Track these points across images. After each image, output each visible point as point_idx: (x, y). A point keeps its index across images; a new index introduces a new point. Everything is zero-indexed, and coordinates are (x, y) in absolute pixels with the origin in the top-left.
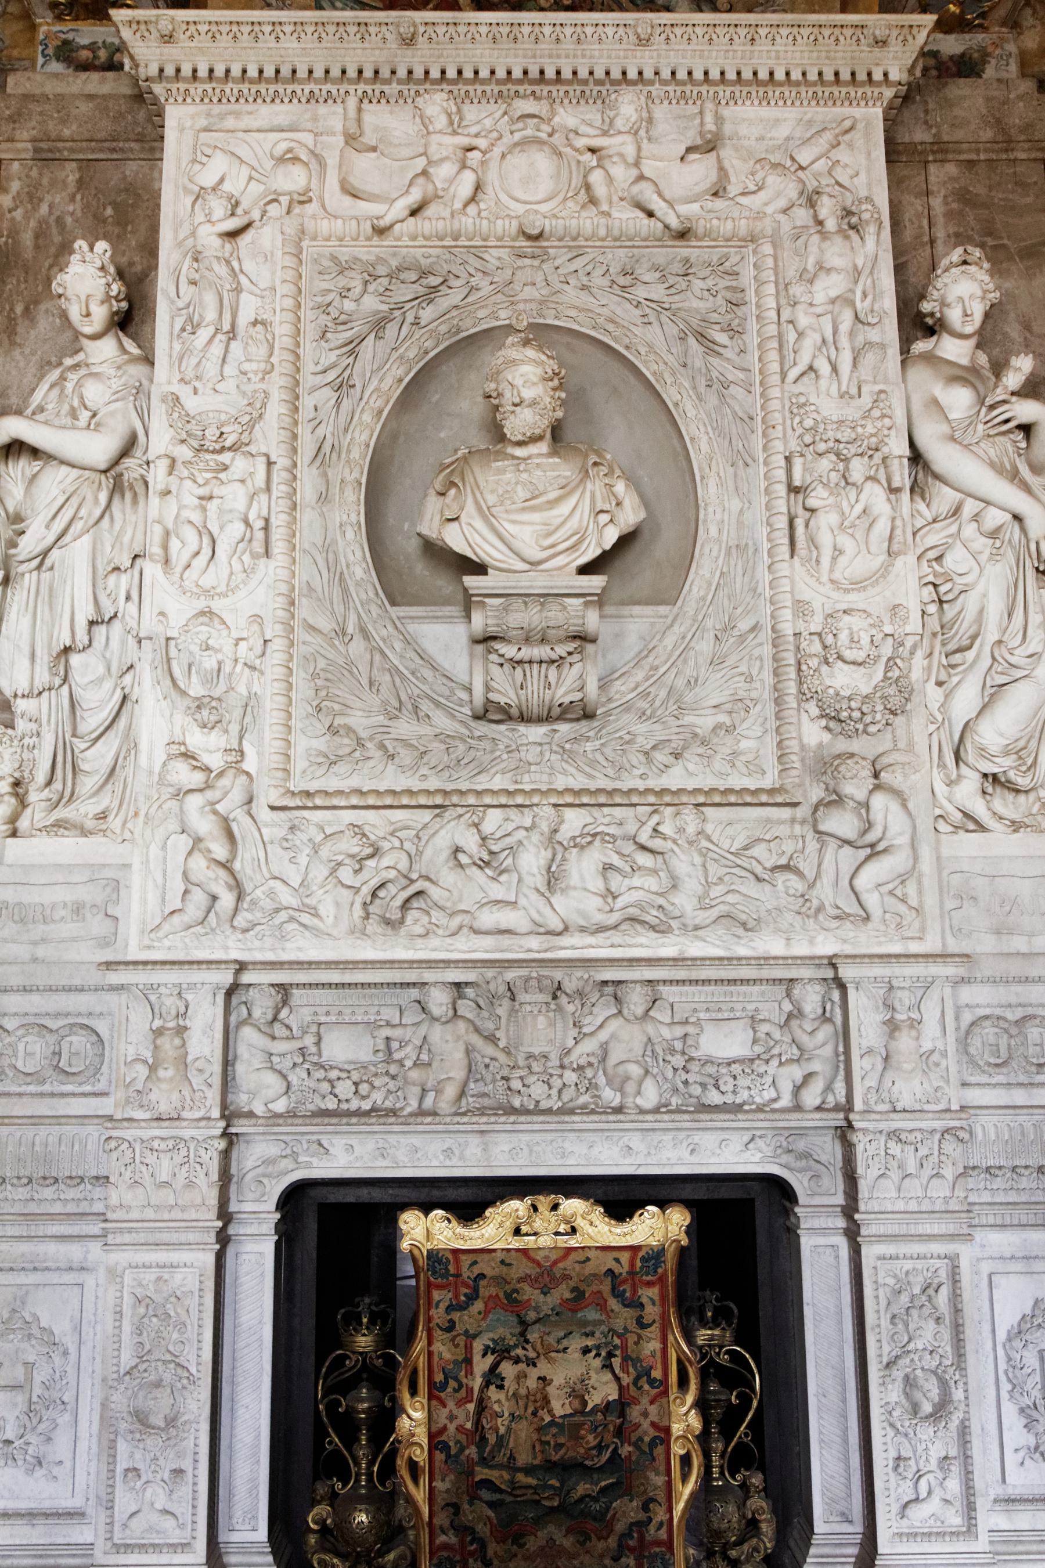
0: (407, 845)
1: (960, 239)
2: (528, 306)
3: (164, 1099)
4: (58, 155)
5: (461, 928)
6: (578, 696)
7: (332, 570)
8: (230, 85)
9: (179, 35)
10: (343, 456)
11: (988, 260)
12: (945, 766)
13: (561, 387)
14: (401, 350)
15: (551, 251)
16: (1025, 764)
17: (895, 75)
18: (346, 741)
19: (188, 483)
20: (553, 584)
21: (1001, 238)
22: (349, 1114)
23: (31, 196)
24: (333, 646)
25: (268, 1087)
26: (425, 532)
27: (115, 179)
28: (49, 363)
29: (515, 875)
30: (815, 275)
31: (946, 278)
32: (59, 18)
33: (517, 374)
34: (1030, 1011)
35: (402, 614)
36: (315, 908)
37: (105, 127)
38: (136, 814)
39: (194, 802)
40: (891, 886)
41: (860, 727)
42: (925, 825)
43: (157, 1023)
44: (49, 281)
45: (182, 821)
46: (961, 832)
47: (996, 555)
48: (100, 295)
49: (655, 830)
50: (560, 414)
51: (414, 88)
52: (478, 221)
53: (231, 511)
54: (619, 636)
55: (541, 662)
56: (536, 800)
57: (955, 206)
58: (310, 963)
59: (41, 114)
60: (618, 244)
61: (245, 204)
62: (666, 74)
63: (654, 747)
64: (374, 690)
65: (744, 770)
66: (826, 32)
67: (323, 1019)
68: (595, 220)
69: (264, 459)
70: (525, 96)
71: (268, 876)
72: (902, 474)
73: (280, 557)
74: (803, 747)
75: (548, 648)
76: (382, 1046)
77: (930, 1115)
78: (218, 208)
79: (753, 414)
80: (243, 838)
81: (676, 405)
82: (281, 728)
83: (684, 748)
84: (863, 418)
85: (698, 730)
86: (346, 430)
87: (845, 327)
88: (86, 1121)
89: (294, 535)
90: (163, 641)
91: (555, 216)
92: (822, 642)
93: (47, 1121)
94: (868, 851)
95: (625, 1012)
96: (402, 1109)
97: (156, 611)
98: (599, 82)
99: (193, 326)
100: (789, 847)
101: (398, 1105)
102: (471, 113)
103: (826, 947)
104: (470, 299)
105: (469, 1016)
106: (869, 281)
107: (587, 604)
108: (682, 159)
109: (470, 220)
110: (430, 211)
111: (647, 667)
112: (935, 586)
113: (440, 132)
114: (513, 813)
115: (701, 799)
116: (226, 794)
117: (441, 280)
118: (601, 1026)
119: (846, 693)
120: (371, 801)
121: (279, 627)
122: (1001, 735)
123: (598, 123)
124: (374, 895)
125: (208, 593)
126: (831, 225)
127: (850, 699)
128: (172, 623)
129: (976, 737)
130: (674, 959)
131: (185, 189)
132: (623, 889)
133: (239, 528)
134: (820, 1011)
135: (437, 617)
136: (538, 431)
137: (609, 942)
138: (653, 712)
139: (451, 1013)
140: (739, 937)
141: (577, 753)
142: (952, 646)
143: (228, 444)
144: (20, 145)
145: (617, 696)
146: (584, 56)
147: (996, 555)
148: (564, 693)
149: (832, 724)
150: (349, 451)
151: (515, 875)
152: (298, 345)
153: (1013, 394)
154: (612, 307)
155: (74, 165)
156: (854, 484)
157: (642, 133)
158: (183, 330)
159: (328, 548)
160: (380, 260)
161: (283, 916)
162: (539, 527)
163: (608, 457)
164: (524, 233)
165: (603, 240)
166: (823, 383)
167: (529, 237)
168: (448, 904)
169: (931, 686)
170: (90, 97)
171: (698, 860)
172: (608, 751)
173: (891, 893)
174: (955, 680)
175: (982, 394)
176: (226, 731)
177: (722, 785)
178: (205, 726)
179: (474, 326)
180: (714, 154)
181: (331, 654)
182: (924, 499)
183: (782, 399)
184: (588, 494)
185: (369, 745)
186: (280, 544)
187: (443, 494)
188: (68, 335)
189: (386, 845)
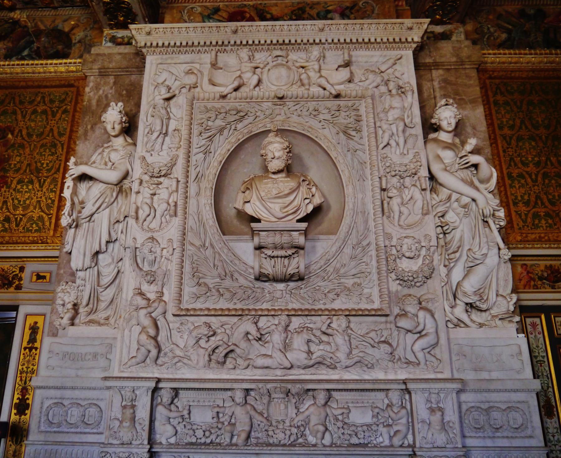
0: (227, 331)
1: (445, 96)
3: (126, 435)
4: (107, 74)
5: (249, 365)
7: (200, 222)
8: (170, 48)
9: (153, 32)
10: (206, 178)
11: (456, 103)
12: (449, 300)
14: (229, 139)
16: (483, 299)
17: (416, 39)
18: (204, 289)
19: (147, 189)
21: (462, 96)
22: (201, 444)
23: (96, 88)
24: (200, 251)
25: (168, 432)
27: (127, 81)
28: (99, 146)
29: (271, 344)
30: (389, 110)
31: (437, 112)
32: (112, 29)
34: (491, 404)
36: (189, 356)
37: (125, 64)
38: (120, 317)
39: (143, 312)
40: (428, 350)
41: (413, 283)
42: (442, 325)
43: (124, 403)
44: (101, 116)
45: (138, 320)
46: (458, 327)
47: (466, 215)
48: (118, 121)
49: (329, 326)
50: (290, 162)
51: (236, 47)
53: (162, 199)
54: (314, 247)
56: (279, 313)
57: (443, 84)
58: (187, 379)
59: (103, 60)
61: (173, 88)
62: (330, 41)
63: (328, 292)
65: (366, 302)
66: (389, 25)
67: (191, 404)
69: (176, 180)
70: (277, 49)
71: (171, 343)
72: (426, 184)
73: (180, 216)
74: (389, 292)
76: (215, 415)
77: (449, 449)
78: (163, 90)
79: (366, 161)
80: (162, 328)
82: (178, 283)
84: (410, 162)
85: (346, 285)
86: (208, 169)
87: (401, 129)
88: (93, 445)
89: (186, 208)
90: (134, 249)
92: (396, 249)
93: (78, 444)
94: (418, 335)
95: (317, 402)
96: (223, 443)
97: (132, 237)
98: (305, 44)
99: (151, 132)
100: (385, 333)
101: (222, 441)
102: (258, 56)
103: (402, 376)
105: (252, 403)
106: (410, 112)
108: (337, 69)
110: (242, 90)
112: (442, 227)
113: (246, 62)
114: (270, 318)
115: (347, 313)
116: (156, 309)
118: (307, 409)
119: (407, 270)
120: (213, 313)
121: (179, 243)
122: (472, 287)
123: (305, 58)
124: (214, 351)
125: (151, 230)
126: (394, 92)
127: (408, 272)
128: (138, 242)
129: (462, 288)
130: (338, 380)
131: (152, 84)
132: (316, 350)
133: (165, 206)
134: (400, 403)
136: (281, 168)
137: (310, 373)
139: (244, 402)
140: (365, 371)
142: (450, 252)
143: (162, 174)
144: (94, 71)
146: (299, 35)
147: (466, 215)
148: (291, 270)
149: (401, 282)
151: (271, 344)
152: (190, 138)
153: (469, 153)
155: (113, 77)
156: (407, 187)
157: (321, 61)
158: (148, 133)
159: (199, 214)
160: (223, 107)
161: (176, 360)
162: (281, 205)
163: (309, 178)
165: (307, 98)
166: (393, 149)
168: (244, 356)
169: (442, 267)
170: (120, 54)
171: (347, 338)
173: (429, 352)
174: (452, 265)
175: (457, 153)
176: (157, 284)
177: (356, 307)
178: (148, 282)
179: (257, 130)
180: (348, 68)
181: (199, 254)
182: (436, 193)
183: (377, 156)
184: (300, 192)
185: (213, 290)
186: (180, 211)
188: (106, 136)
189: (219, 331)
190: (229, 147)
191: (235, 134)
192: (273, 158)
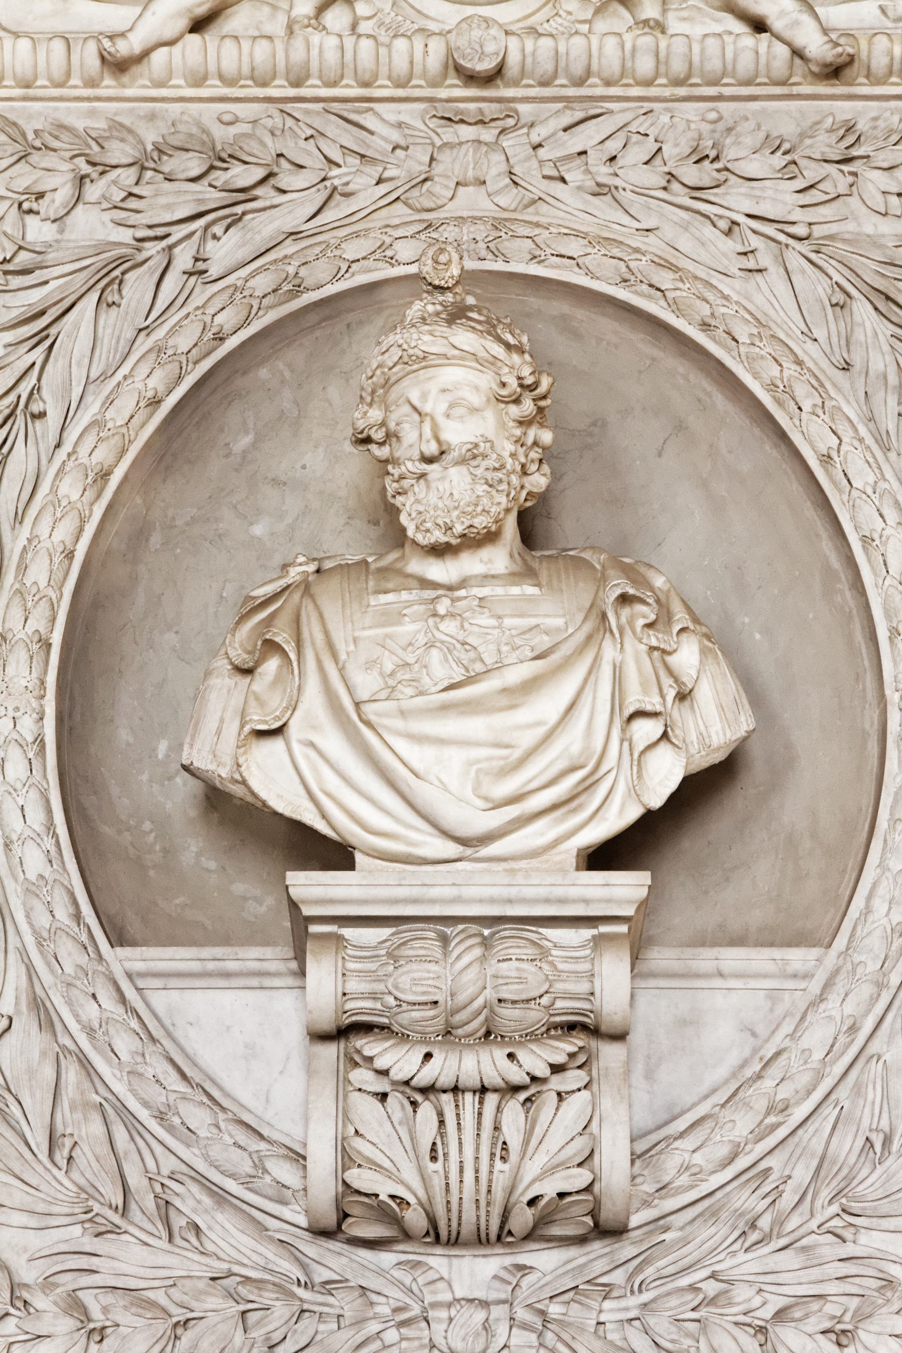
2: (466, 233)
6: (580, 1178)
13: (540, 416)
15: (523, 108)
20: (513, 892)
26: (202, 762)
33: (433, 387)
35: (139, 966)
50: (539, 481)
52: (349, 42)
55: (483, 1090)
60: (682, 91)
63: (780, 1315)
64: (61, 1160)
68: (628, 38)
75: (500, 1054)
81: (826, 459)
83: (861, 1317)
91: (533, 31)
104: (328, 216)
107: (598, 941)
109: (333, 41)
111: (761, 1105)
117: (260, 173)
135: (227, 975)
136: (481, 522)
138: (779, 1222)
141: (582, 1329)
145: (684, 1179)
150: (23, 568)
154: (668, 231)
160: (119, 130)
163: (659, 582)
164: (459, 70)
167: (470, 78)
172: (660, 1324)
179: (336, 277)
187: (248, 672)
190: (157, 382)
191: (197, 300)
192: (429, 460)
